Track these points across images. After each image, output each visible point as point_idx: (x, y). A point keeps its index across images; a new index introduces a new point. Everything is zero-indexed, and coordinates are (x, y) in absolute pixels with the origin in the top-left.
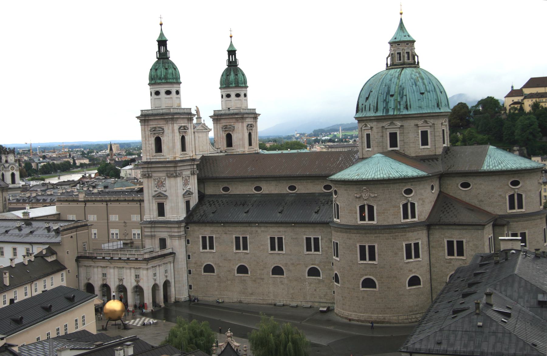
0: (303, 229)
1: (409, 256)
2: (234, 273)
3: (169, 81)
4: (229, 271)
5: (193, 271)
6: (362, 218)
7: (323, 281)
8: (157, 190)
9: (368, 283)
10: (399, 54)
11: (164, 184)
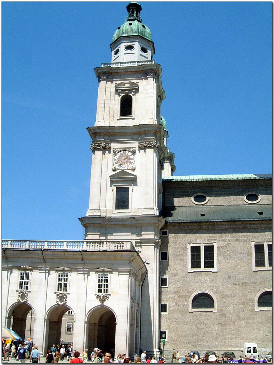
4: (243, 303)
5: (170, 307)
8: (117, 167)
11: (133, 159)
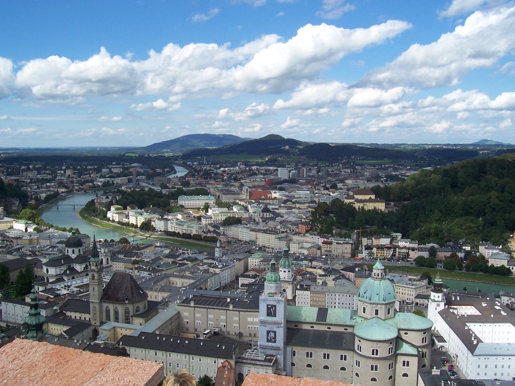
1: (389, 369)
6: (373, 354)
7: (347, 373)
9: (373, 380)
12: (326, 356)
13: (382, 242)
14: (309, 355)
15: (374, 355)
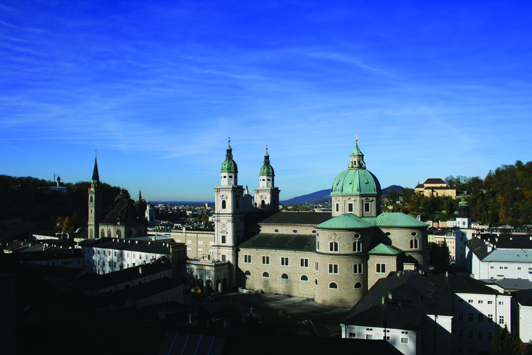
0: (299, 254)
1: (355, 272)
2: (261, 276)
3: (231, 171)
4: (259, 275)
6: (331, 250)
7: (309, 283)
8: (222, 228)
9: (333, 285)
10: (355, 162)
12: (285, 262)
13: (449, 224)
14: (266, 260)
15: (332, 250)
